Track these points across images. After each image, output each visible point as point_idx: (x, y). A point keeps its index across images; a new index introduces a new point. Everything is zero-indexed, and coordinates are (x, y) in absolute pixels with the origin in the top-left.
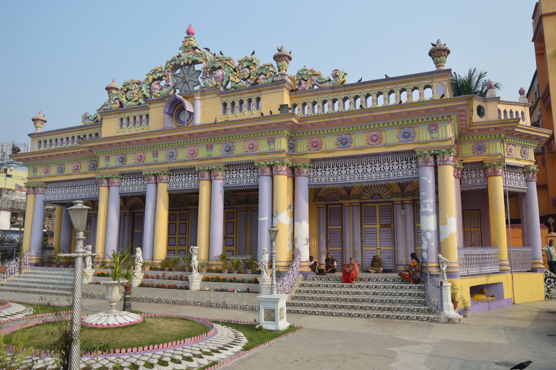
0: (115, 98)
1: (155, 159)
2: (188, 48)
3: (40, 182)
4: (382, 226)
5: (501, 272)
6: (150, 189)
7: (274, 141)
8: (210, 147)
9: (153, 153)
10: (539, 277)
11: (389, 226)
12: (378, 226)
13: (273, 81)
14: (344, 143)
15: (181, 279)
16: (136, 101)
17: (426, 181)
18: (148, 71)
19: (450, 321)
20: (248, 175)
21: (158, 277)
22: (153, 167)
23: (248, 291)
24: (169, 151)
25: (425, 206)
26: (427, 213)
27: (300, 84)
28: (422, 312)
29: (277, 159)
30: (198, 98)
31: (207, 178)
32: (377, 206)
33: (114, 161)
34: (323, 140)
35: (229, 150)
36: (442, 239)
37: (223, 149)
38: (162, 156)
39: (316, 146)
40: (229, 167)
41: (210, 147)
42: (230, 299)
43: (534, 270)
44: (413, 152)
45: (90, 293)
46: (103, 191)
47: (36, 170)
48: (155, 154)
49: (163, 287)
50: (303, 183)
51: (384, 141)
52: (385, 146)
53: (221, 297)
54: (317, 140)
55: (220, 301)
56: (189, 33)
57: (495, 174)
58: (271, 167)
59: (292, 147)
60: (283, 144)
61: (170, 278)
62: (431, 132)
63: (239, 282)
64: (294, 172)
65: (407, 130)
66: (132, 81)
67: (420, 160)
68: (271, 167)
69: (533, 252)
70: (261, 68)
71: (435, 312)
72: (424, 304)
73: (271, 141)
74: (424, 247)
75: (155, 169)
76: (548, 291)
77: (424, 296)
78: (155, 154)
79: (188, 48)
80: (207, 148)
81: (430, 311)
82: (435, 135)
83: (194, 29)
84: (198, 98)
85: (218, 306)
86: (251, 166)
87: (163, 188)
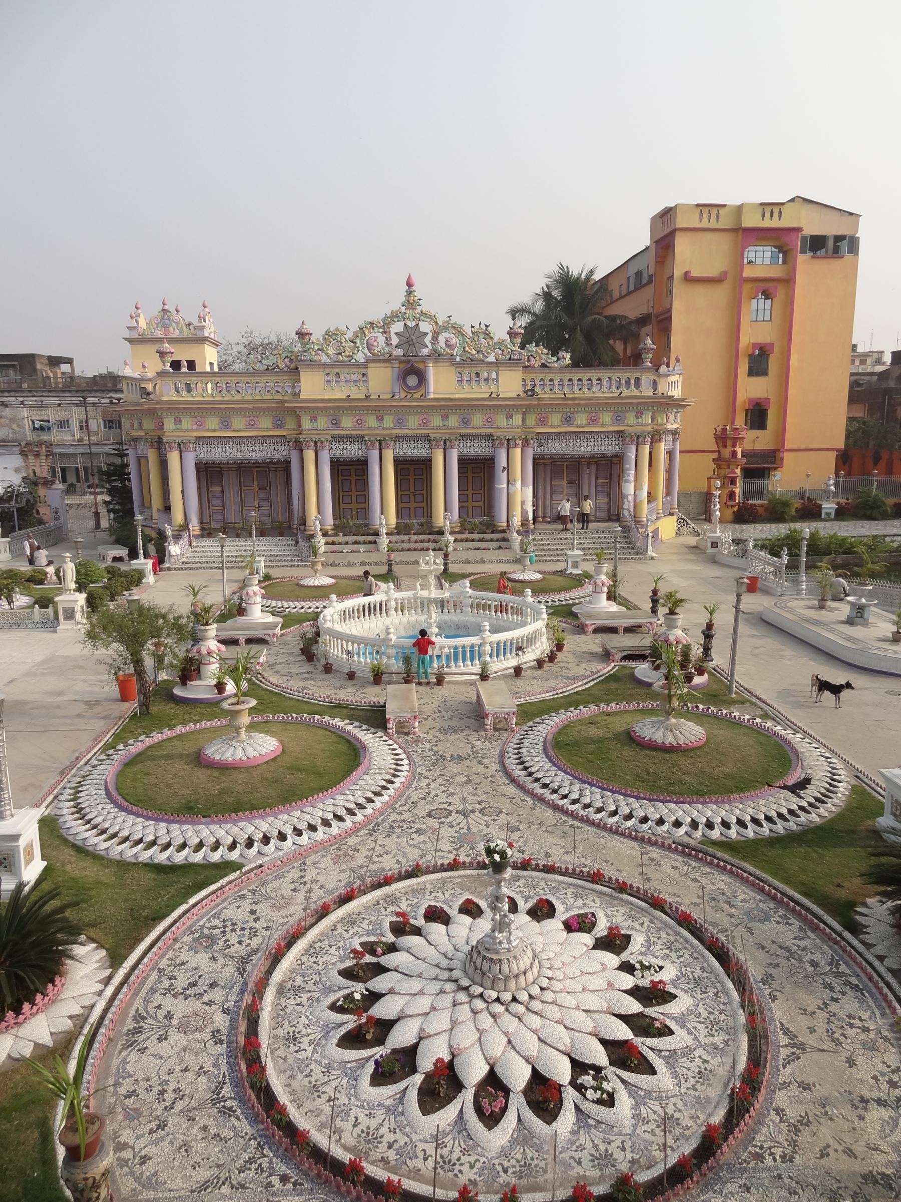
0: (316, 347)
1: (380, 424)
2: (411, 302)
3: (191, 437)
4: (568, 482)
5: (658, 518)
6: (374, 454)
7: (512, 417)
8: (445, 417)
9: (377, 418)
10: (675, 518)
11: (574, 482)
12: (565, 482)
13: (510, 359)
14: (568, 420)
15: (435, 542)
16: (349, 356)
17: (630, 457)
18: (361, 323)
19: (652, 558)
20: (483, 445)
21: (403, 542)
22: (378, 432)
23: (500, 548)
24: (397, 418)
25: (629, 476)
26: (629, 481)
27: (529, 360)
28: (633, 554)
29: (516, 434)
30: (431, 365)
31: (442, 446)
32: (565, 464)
33: (322, 422)
34: (550, 416)
35: (465, 422)
36: (638, 501)
37: (460, 420)
38: (388, 421)
39: (542, 421)
40: (464, 437)
41: (445, 417)
42: (487, 555)
43: (671, 514)
44: (621, 432)
45: (331, 561)
46: (310, 455)
47: (180, 420)
48: (380, 419)
49: (415, 550)
50: (530, 452)
51: (601, 422)
52: (602, 426)
53: (478, 555)
54: (545, 416)
55: (478, 558)
56: (409, 284)
57: (660, 440)
58: (508, 440)
59: (523, 420)
60: (517, 420)
61: (416, 542)
62: (637, 418)
63: (487, 541)
64: (526, 444)
65: (619, 414)
66: (337, 329)
67: (628, 440)
68: (508, 440)
69: (672, 500)
70: (498, 343)
71: (641, 554)
72: (632, 548)
73: (509, 417)
74: (626, 506)
75: (381, 434)
76: (679, 530)
77: (630, 543)
78: (380, 419)
79: (411, 302)
80: (442, 417)
81: (637, 553)
82: (640, 421)
83: (415, 280)
84: (431, 365)
85: (476, 562)
86: (489, 437)
87: (389, 455)
